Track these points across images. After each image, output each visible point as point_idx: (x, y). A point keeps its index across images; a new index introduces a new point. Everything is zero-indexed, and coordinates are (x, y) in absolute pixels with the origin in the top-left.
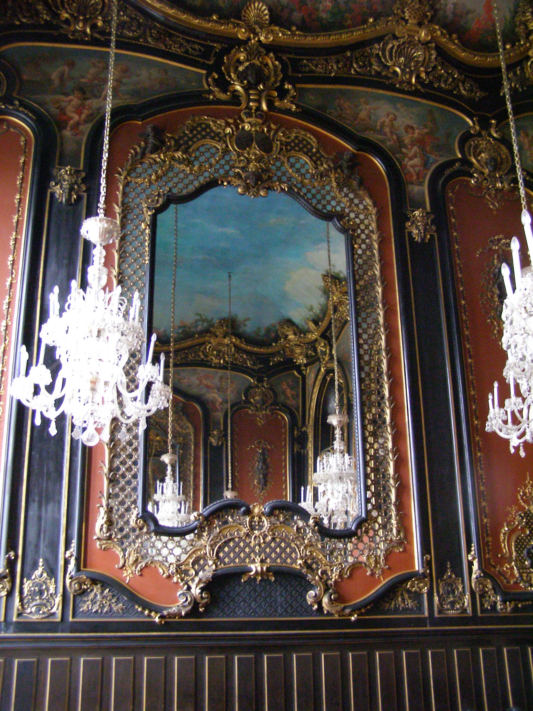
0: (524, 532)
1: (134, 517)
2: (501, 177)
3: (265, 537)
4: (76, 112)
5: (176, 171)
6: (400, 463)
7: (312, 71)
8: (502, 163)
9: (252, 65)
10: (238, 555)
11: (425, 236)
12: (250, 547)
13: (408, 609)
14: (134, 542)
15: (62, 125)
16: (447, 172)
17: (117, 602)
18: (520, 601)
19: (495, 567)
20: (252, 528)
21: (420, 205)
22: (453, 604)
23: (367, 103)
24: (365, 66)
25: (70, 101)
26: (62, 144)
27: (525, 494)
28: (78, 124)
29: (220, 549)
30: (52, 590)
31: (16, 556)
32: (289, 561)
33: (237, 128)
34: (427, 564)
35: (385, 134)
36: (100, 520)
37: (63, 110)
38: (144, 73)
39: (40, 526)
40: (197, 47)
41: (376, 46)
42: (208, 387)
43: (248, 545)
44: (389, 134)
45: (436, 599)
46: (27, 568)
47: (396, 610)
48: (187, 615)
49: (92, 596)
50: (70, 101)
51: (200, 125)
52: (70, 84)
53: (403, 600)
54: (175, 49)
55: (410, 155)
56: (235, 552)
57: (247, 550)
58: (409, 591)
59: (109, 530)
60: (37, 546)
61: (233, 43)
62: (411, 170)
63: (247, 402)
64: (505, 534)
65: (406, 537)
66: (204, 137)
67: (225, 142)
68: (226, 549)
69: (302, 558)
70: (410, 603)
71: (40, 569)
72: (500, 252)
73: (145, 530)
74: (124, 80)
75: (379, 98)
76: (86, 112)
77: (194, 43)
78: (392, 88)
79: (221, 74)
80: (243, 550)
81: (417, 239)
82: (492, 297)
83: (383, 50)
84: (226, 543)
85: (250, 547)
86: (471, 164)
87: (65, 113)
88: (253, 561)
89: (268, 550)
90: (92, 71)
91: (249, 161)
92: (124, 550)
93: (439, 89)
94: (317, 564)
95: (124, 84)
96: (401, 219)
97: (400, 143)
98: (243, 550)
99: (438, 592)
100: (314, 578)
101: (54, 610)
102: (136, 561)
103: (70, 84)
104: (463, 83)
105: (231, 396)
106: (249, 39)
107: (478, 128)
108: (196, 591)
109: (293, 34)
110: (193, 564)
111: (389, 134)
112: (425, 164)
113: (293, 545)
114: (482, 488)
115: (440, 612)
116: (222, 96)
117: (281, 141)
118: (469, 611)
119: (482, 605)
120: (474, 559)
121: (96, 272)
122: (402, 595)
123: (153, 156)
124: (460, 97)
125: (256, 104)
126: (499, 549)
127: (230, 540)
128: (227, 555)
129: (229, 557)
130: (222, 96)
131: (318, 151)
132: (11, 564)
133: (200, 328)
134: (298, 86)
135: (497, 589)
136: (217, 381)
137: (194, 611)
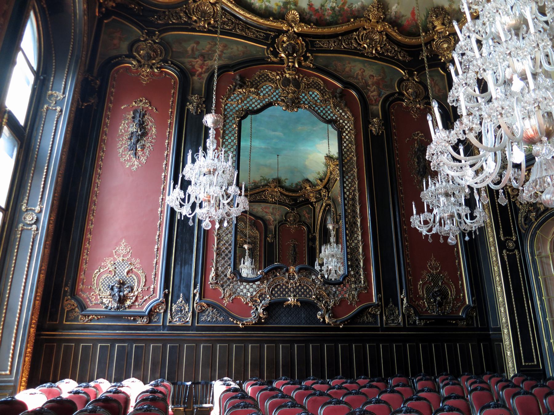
0: (431, 284)
1: (229, 272)
2: (419, 101)
3: (296, 283)
4: (200, 68)
5: (251, 98)
6: (366, 248)
8: (419, 94)
10: (282, 293)
11: (379, 132)
12: (288, 289)
13: (369, 322)
14: (229, 285)
15: (193, 74)
16: (391, 99)
17: (220, 316)
18: (429, 319)
19: (415, 302)
21: (377, 116)
22: (393, 320)
23: (349, 63)
24: (349, 44)
25: (197, 61)
26: (193, 84)
27: (431, 264)
28: (201, 73)
29: (273, 289)
30: (187, 310)
31: (169, 292)
32: (308, 296)
33: (283, 76)
34: (379, 299)
35: (359, 80)
36: (212, 274)
37: (193, 66)
38: (235, 48)
39: (181, 277)
41: (355, 33)
42: (266, 212)
43: (287, 287)
44: (361, 80)
45: (384, 317)
46: (174, 298)
47: (363, 323)
49: (207, 313)
50: (197, 61)
51: (263, 75)
52: (197, 53)
53: (367, 318)
54: (250, 35)
55: (372, 90)
56: (280, 291)
57: (287, 290)
58: (370, 313)
59: (216, 279)
60: (180, 287)
61: (280, 32)
62: (372, 98)
63: (286, 220)
65: (368, 285)
66: (265, 81)
67: (276, 83)
68: (276, 289)
69: (314, 295)
70: (371, 319)
71: (181, 299)
73: (235, 279)
74: (225, 51)
75: (355, 61)
76: (205, 67)
77: (260, 32)
78: (362, 55)
80: (284, 290)
82: (414, 163)
83: (358, 36)
84: (276, 286)
85: (288, 289)
86: (404, 95)
87: (194, 68)
88: (290, 296)
89: (297, 290)
90: (208, 46)
91: (288, 93)
92: (224, 290)
93: (388, 56)
94: (322, 298)
95: (225, 53)
96: (367, 122)
98: (284, 290)
99: (385, 314)
100: (321, 305)
101: (188, 320)
102: (230, 295)
103: (197, 53)
104: (400, 52)
105: (278, 217)
106: (289, 30)
107: (407, 76)
108: (260, 310)
109: (312, 28)
110: (259, 297)
111: (361, 80)
112: (379, 95)
113: (310, 288)
114: (408, 261)
115: (386, 324)
117: (305, 83)
118: (402, 324)
119: (408, 321)
120: (404, 297)
121: (211, 143)
122: (366, 315)
123: (239, 90)
124: (398, 60)
125: (292, 64)
127: (278, 285)
128: (277, 292)
129: (278, 294)
131: (324, 88)
132: (166, 296)
133: (263, 183)
134: (314, 54)
135: (416, 313)
136: (271, 210)
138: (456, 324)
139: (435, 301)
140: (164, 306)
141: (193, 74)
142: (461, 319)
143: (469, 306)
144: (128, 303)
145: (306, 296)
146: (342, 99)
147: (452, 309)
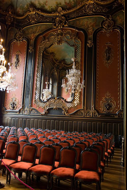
7: (71, 17)
9: (59, 20)
20: (55, 101)
23: (82, 20)
24: (82, 13)
30: (28, 110)
35: (85, 26)
37: (31, 37)
40: (51, 19)
43: (54, 104)
44: (86, 26)
46: (25, 107)
47: (78, 115)
48: (44, 114)
51: (51, 34)
54: (48, 21)
55: (90, 29)
58: (80, 112)
59: (35, 101)
61: (57, 16)
62: (90, 32)
64: (101, 102)
66: (52, 36)
67: (55, 36)
72: (108, 45)
78: (88, 15)
79: (55, 23)
81: (89, 47)
86: (104, 28)
87: (31, 37)
93: (98, 12)
96: (86, 43)
97: (88, 27)
100: (64, 109)
102: (38, 106)
109: (66, 11)
111: (86, 26)
116: (55, 27)
124: (103, 12)
126: (100, 105)
130: (55, 27)
132: (23, 106)
134: (69, 21)
137: (46, 113)
138: (114, 117)
139: (106, 109)
140: (22, 109)
141: (31, 40)
142: (116, 115)
143: (121, 110)
144: (15, 108)
145: (60, 106)
146: (78, 35)
147: (113, 111)
